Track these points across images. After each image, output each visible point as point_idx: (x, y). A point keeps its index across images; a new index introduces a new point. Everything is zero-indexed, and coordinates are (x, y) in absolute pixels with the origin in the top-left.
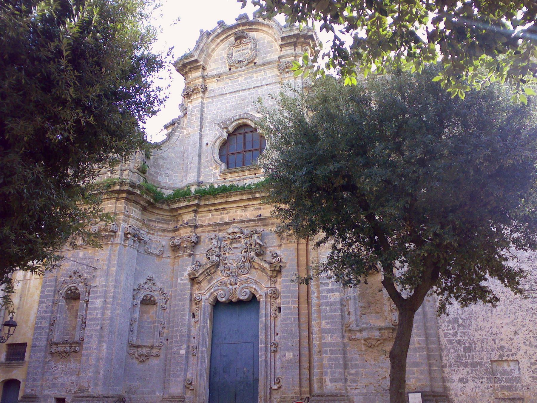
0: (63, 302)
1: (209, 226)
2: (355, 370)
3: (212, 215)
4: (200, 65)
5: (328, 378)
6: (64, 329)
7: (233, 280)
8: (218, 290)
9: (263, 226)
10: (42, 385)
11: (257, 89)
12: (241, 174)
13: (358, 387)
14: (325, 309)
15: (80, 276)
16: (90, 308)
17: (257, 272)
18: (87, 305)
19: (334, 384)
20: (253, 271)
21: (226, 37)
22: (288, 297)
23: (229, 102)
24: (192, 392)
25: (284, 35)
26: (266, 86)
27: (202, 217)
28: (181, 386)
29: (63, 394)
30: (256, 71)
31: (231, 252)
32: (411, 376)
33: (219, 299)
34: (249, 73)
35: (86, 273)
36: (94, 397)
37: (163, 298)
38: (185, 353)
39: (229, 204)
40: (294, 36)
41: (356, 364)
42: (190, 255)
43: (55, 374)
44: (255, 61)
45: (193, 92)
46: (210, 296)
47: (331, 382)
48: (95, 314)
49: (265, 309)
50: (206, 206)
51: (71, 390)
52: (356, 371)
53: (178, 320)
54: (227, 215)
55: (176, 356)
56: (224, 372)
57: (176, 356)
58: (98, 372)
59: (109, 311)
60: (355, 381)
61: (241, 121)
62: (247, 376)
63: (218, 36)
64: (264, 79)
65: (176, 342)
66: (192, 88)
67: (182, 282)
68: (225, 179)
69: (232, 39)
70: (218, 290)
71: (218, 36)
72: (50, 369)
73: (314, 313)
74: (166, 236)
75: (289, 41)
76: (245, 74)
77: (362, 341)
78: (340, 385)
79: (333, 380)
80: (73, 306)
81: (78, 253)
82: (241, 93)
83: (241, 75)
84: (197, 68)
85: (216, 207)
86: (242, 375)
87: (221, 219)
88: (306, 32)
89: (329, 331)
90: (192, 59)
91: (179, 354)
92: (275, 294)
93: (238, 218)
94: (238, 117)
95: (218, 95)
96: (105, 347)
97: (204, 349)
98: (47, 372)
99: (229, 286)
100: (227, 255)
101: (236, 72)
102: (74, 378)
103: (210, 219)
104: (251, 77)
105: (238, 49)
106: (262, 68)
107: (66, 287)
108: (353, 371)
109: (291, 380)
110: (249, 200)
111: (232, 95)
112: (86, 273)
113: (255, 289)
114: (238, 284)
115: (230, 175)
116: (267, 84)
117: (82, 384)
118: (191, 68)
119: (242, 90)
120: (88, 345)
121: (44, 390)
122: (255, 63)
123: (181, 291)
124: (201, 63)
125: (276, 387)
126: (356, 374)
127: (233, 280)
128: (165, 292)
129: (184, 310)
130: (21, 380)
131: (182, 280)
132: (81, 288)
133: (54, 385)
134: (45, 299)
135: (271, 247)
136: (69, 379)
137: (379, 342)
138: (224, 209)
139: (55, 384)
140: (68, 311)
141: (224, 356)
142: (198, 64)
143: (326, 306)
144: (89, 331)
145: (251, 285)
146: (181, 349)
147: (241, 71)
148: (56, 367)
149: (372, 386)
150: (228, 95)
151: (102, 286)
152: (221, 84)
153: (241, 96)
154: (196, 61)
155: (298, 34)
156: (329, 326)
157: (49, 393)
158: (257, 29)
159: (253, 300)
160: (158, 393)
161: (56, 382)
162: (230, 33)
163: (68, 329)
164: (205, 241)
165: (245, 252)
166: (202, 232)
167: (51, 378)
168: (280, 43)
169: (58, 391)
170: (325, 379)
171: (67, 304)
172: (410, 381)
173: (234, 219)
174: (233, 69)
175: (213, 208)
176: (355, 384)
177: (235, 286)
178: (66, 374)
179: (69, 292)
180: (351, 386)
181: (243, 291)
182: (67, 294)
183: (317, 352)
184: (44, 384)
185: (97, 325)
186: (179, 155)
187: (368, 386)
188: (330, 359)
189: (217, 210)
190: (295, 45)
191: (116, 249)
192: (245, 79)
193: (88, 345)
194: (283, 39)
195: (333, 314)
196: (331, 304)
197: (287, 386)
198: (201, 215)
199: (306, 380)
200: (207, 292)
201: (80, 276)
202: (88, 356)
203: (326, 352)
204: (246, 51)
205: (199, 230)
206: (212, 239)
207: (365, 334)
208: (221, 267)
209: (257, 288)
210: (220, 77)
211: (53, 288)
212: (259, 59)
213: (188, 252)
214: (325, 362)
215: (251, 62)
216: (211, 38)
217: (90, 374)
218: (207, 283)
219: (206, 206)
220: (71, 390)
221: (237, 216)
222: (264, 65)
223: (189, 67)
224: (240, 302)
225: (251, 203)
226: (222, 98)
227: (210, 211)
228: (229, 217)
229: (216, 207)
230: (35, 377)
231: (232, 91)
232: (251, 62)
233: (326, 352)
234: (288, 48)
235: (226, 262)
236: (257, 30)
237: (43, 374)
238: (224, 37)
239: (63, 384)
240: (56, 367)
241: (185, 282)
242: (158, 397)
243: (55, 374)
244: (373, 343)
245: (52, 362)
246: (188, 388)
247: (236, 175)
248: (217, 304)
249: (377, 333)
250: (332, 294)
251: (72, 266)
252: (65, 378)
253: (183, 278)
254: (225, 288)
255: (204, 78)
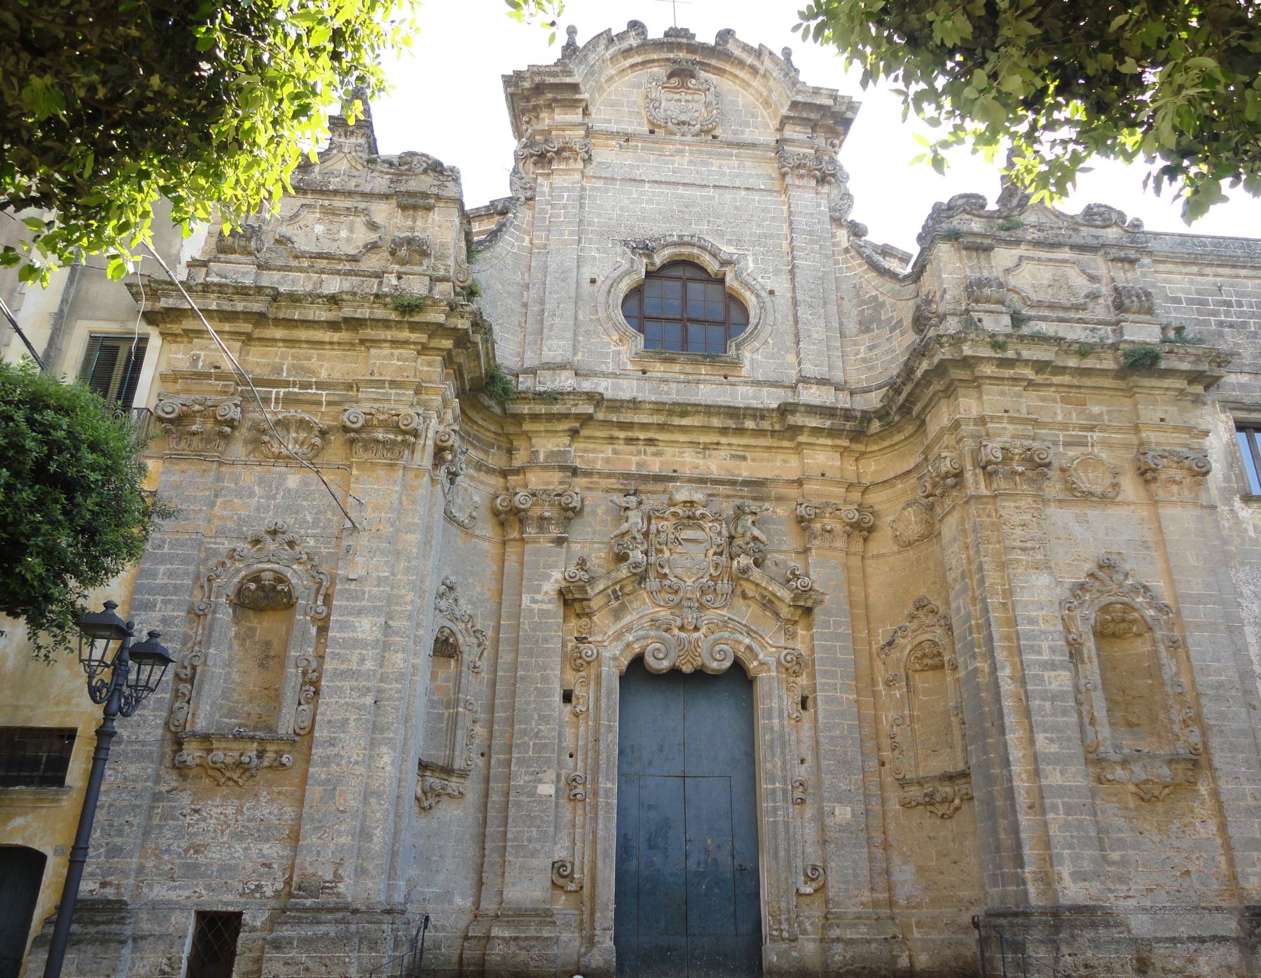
0: (225, 614)
1: (610, 476)
2: (1118, 853)
3: (615, 452)
4: (581, 101)
5: (1065, 871)
6: (224, 695)
7: (690, 617)
8: (644, 638)
9: (754, 499)
10: (141, 869)
11: (721, 191)
12: (688, 368)
13: (1130, 894)
14: (1041, 708)
15: (291, 544)
16: (335, 639)
17: (749, 606)
18: (323, 630)
19: (1082, 884)
20: (740, 602)
21: (644, 63)
22: (834, 675)
23: (650, 201)
24: (573, 897)
25: (800, 98)
26: (743, 193)
27: (585, 451)
28: (545, 879)
29: (228, 897)
30: (719, 154)
31: (680, 549)
32: (1248, 870)
33: (649, 660)
34: (701, 152)
35: (314, 536)
36: (355, 911)
37: (475, 641)
38: (552, 792)
39: (668, 431)
40: (820, 107)
41: (1119, 840)
42: (560, 541)
43: (195, 834)
44: (716, 133)
45: (558, 153)
46: (623, 651)
47: (1074, 881)
48: (355, 659)
49: (774, 699)
50: (607, 423)
51: (259, 887)
52: (1123, 856)
53: (528, 703)
54: (657, 460)
55: (524, 799)
56: (651, 847)
57: (524, 799)
58: (364, 834)
59: (400, 655)
60: (1121, 879)
61: (684, 250)
62: (715, 860)
63: (627, 52)
64: (738, 175)
65: (521, 762)
66: (557, 145)
67: (535, 606)
68: (644, 372)
69: (660, 71)
70: (644, 638)
71: (627, 52)
72: (173, 818)
73: (1009, 715)
74: (482, 483)
75: (805, 115)
76: (691, 153)
77: (1132, 788)
78: (1095, 887)
79: (1078, 876)
80: (253, 630)
81: (282, 478)
82: (681, 190)
83: (680, 152)
84: (574, 104)
85: (630, 434)
86: (702, 857)
87: (639, 465)
88: (844, 108)
89: (1057, 760)
90: (568, 80)
91: (532, 794)
92: (795, 665)
93: (687, 472)
94: (675, 239)
95: (622, 179)
96: (387, 759)
97: (609, 785)
98: (160, 827)
99: (676, 631)
100: (667, 554)
101: (665, 142)
102: (272, 850)
103: (607, 461)
104: (705, 164)
105: (677, 97)
106: (735, 151)
107: (241, 571)
108: (1115, 856)
109: (850, 871)
110: (724, 431)
111: (658, 189)
112: (314, 536)
113: (749, 648)
114: (703, 630)
115: (659, 366)
116: (748, 189)
117: (311, 870)
118: (555, 100)
119: (685, 184)
120: (331, 751)
121: (151, 887)
122: (714, 137)
123: (534, 630)
124: (586, 96)
125: (809, 890)
126: (1123, 862)
127: (690, 617)
128: (478, 627)
129: (545, 679)
130: (48, 850)
131: (534, 601)
132: (297, 577)
133: (192, 870)
134: (159, 598)
135: (778, 551)
136: (254, 851)
137: (1167, 791)
138: (651, 442)
139: (196, 866)
140: (235, 642)
141: (650, 807)
142: (577, 97)
143: (1043, 700)
144: (329, 708)
145: (740, 637)
146: (540, 781)
147: (682, 143)
148: (197, 811)
149: (1163, 893)
150: (647, 185)
151: (380, 581)
152: (628, 158)
153: (682, 196)
154: (575, 87)
155: (829, 107)
156: (1054, 748)
157: (173, 895)
158: (719, 69)
159: (739, 677)
160: (458, 901)
161: (201, 859)
162: (656, 57)
163: (236, 696)
164: (594, 513)
165: (715, 554)
166: (588, 488)
167: (178, 846)
168: (784, 111)
169: (208, 887)
170: (1059, 873)
171: (237, 619)
172: (1248, 882)
173: (675, 471)
174: (660, 133)
175: (622, 435)
176: (1124, 888)
177: (696, 635)
178: (239, 836)
179: (253, 586)
180: (1116, 890)
181: (717, 648)
182: (240, 591)
183: (1024, 807)
184: (150, 864)
185: (365, 691)
186: (511, 290)
187: (1151, 890)
188: (1066, 826)
189: (630, 441)
190: (814, 126)
191: (416, 483)
192: (690, 162)
193: (331, 751)
194: (795, 105)
195: (1060, 719)
196: (1053, 698)
197: (843, 886)
198: (582, 445)
199: (880, 874)
200: (613, 642)
201: (291, 544)
202: (332, 787)
203: (1054, 808)
204: (696, 106)
205: (581, 481)
206: (627, 509)
207: (1139, 772)
208: (652, 583)
209: (754, 646)
210: (627, 140)
211: (192, 568)
212: (724, 132)
213: (554, 531)
214: (1054, 831)
215: (707, 132)
216: (612, 50)
217: (343, 840)
218: (612, 619)
219: (607, 423)
220: (259, 887)
221: (683, 464)
222: (729, 144)
223: (550, 96)
224: (701, 679)
225: (724, 440)
226: (629, 187)
227: (612, 440)
228: (662, 464)
229: (630, 434)
230: (118, 841)
231: (657, 178)
232: (707, 132)
233: (1054, 808)
234: (798, 128)
235: (666, 570)
236: (720, 71)
237: (146, 834)
238: (639, 59)
239: (225, 869)
240: (197, 811)
241: (545, 607)
242: (461, 911)
243: (195, 834)
244: (1156, 793)
245: (184, 794)
246: (562, 888)
247: (677, 368)
248: (636, 671)
249: (1165, 771)
250: (1053, 674)
251: (258, 510)
252: (239, 847)
253: (539, 597)
254: (667, 635)
255: (589, 133)
